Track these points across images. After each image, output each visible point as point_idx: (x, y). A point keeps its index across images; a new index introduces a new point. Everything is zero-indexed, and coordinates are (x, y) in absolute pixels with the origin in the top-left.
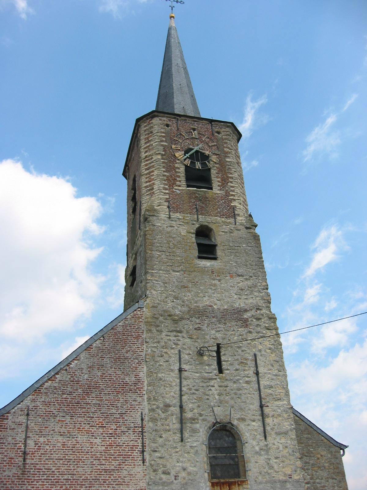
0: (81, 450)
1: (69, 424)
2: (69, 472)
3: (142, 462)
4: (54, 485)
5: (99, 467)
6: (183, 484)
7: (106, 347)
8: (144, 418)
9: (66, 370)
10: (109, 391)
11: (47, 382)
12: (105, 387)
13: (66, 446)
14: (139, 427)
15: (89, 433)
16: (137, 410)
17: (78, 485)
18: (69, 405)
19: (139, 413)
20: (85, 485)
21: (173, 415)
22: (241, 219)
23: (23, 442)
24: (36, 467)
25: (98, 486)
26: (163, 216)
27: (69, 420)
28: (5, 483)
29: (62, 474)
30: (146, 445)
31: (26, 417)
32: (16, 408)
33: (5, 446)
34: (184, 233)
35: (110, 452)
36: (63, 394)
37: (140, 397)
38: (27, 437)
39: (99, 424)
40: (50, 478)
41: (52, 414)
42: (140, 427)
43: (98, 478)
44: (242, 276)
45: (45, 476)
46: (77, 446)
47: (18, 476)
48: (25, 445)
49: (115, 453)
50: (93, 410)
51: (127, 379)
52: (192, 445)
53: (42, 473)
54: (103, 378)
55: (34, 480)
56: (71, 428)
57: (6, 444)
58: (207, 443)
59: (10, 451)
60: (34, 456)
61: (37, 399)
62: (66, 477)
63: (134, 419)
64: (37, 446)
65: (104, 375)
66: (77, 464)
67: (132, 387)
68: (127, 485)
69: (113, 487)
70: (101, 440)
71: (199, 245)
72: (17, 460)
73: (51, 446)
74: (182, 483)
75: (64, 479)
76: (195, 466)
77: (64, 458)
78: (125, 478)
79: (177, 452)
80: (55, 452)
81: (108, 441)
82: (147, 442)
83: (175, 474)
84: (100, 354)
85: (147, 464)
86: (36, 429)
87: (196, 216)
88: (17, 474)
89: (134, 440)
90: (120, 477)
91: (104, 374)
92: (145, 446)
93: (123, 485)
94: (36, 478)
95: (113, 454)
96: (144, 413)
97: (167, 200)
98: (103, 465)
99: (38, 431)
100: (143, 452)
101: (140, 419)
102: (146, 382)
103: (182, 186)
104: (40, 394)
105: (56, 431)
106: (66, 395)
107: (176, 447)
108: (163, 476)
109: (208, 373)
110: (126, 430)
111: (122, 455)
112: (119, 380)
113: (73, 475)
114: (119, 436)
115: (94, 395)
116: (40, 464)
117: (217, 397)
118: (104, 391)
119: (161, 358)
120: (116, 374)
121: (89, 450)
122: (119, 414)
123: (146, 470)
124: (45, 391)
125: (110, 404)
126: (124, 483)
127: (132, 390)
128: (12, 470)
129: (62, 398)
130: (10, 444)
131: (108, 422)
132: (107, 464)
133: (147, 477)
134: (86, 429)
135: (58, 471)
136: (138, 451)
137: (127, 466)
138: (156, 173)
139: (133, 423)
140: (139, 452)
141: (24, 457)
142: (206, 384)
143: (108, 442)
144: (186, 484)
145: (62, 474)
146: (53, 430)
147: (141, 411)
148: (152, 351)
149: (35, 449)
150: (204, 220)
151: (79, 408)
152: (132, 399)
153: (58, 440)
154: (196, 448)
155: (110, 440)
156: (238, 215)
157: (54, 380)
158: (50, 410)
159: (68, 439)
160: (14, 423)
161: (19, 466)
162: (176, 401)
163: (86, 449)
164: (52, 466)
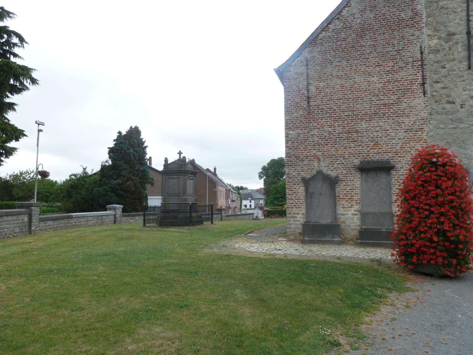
0: (359, 89)
1: (345, 68)
2: (349, 109)
3: (422, 94)
4: (336, 121)
5: (378, 102)
8: (423, 51)
9: (338, 18)
10: (384, 31)
11: (320, 33)
12: (379, 27)
13: (344, 87)
14: (418, 61)
15: (366, 73)
16: (416, 44)
17: (358, 119)
18: (344, 51)
19: (418, 47)
20: (365, 119)
21: (457, 43)
23: (306, 89)
24: (319, 107)
25: (378, 119)
28: (294, 122)
29: (343, 112)
30: (427, 77)
31: (305, 67)
32: (296, 61)
33: (291, 93)
35: (388, 87)
36: (337, 41)
37: (418, 30)
38: (308, 84)
39: (375, 64)
40: (333, 115)
41: (329, 61)
42: (420, 61)
43: (377, 112)
45: (328, 114)
46: (355, 86)
47: (305, 117)
48: (308, 90)
49: (393, 88)
50: (368, 52)
51: (403, 15)
53: (324, 112)
54: (376, 19)
55: (319, 118)
56: (347, 71)
57: (292, 92)
59: (296, 97)
60: (317, 99)
61: (314, 50)
62: (347, 114)
63: (413, 54)
64: (318, 90)
65: (377, 16)
66: (356, 102)
67: (408, 22)
68: (407, 116)
69: (393, 119)
70: (378, 78)
72: (302, 104)
73: (331, 89)
75: (345, 116)
77: (343, 98)
78: (405, 110)
79: (464, 81)
80: (334, 93)
81: (386, 78)
82: (428, 74)
83: (461, 103)
85: (429, 95)
86: (316, 76)
88: (304, 115)
89: (413, 74)
90: (400, 109)
91: (378, 15)
92: (426, 79)
93: (403, 116)
94: (320, 117)
96: (423, 47)
98: (382, 100)
99: (318, 77)
100: (423, 84)
101: (419, 52)
102: (425, 14)
104: (316, 46)
105: (334, 74)
106: (340, 42)
107: (462, 76)
108: (448, 106)
110: (404, 65)
111: (401, 89)
112: (393, 17)
113: (353, 111)
114: (397, 72)
115: (368, 37)
116: (322, 105)
118: (378, 32)
120: (390, 13)
121: (366, 88)
122: (395, 51)
123: (427, 101)
124: (321, 41)
125: (385, 43)
126: (404, 115)
127: (409, 25)
128: (299, 112)
129: (337, 45)
130: (295, 91)
131: (385, 60)
132: (385, 99)
133: (429, 108)
134: (362, 70)
135: (339, 109)
136: (418, 84)
137: (407, 99)
140: (419, 85)
141: (308, 100)
143: (385, 79)
145: (343, 112)
146: (331, 75)
147: (420, 44)
149: (316, 93)
151: (354, 51)
152: (409, 35)
153: (336, 83)
155: (388, 77)
157: (327, 31)
158: (326, 58)
159: (346, 81)
160: (296, 74)
161: (304, 109)
164: (333, 105)
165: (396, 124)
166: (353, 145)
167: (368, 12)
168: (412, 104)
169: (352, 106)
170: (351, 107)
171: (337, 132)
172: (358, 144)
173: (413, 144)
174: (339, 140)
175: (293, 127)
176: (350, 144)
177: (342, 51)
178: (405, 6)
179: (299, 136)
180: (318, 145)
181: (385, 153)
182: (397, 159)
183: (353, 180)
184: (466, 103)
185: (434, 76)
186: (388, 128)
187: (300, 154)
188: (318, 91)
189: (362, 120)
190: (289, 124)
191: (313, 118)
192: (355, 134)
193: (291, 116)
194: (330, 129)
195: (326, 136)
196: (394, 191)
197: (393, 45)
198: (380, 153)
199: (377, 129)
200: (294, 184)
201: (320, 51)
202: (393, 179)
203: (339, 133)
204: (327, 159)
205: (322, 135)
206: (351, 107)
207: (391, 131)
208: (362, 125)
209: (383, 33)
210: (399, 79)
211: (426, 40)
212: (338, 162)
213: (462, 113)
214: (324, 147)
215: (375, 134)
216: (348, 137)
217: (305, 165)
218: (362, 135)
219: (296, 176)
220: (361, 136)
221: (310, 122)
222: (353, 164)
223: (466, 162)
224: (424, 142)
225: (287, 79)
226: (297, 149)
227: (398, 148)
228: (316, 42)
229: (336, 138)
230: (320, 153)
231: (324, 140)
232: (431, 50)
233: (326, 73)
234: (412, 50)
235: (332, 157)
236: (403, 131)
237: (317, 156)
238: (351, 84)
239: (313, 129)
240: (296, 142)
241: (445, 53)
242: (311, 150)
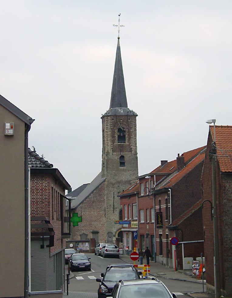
22: (133, 152)
26: (111, 154)
34: (116, 158)
38: (81, 213)
44: (131, 170)
71: (120, 162)
87: (120, 153)
97: (112, 149)
100: (105, 215)
103: (116, 143)
138: (109, 139)
150: (122, 154)
156: (132, 151)
162: (113, 204)
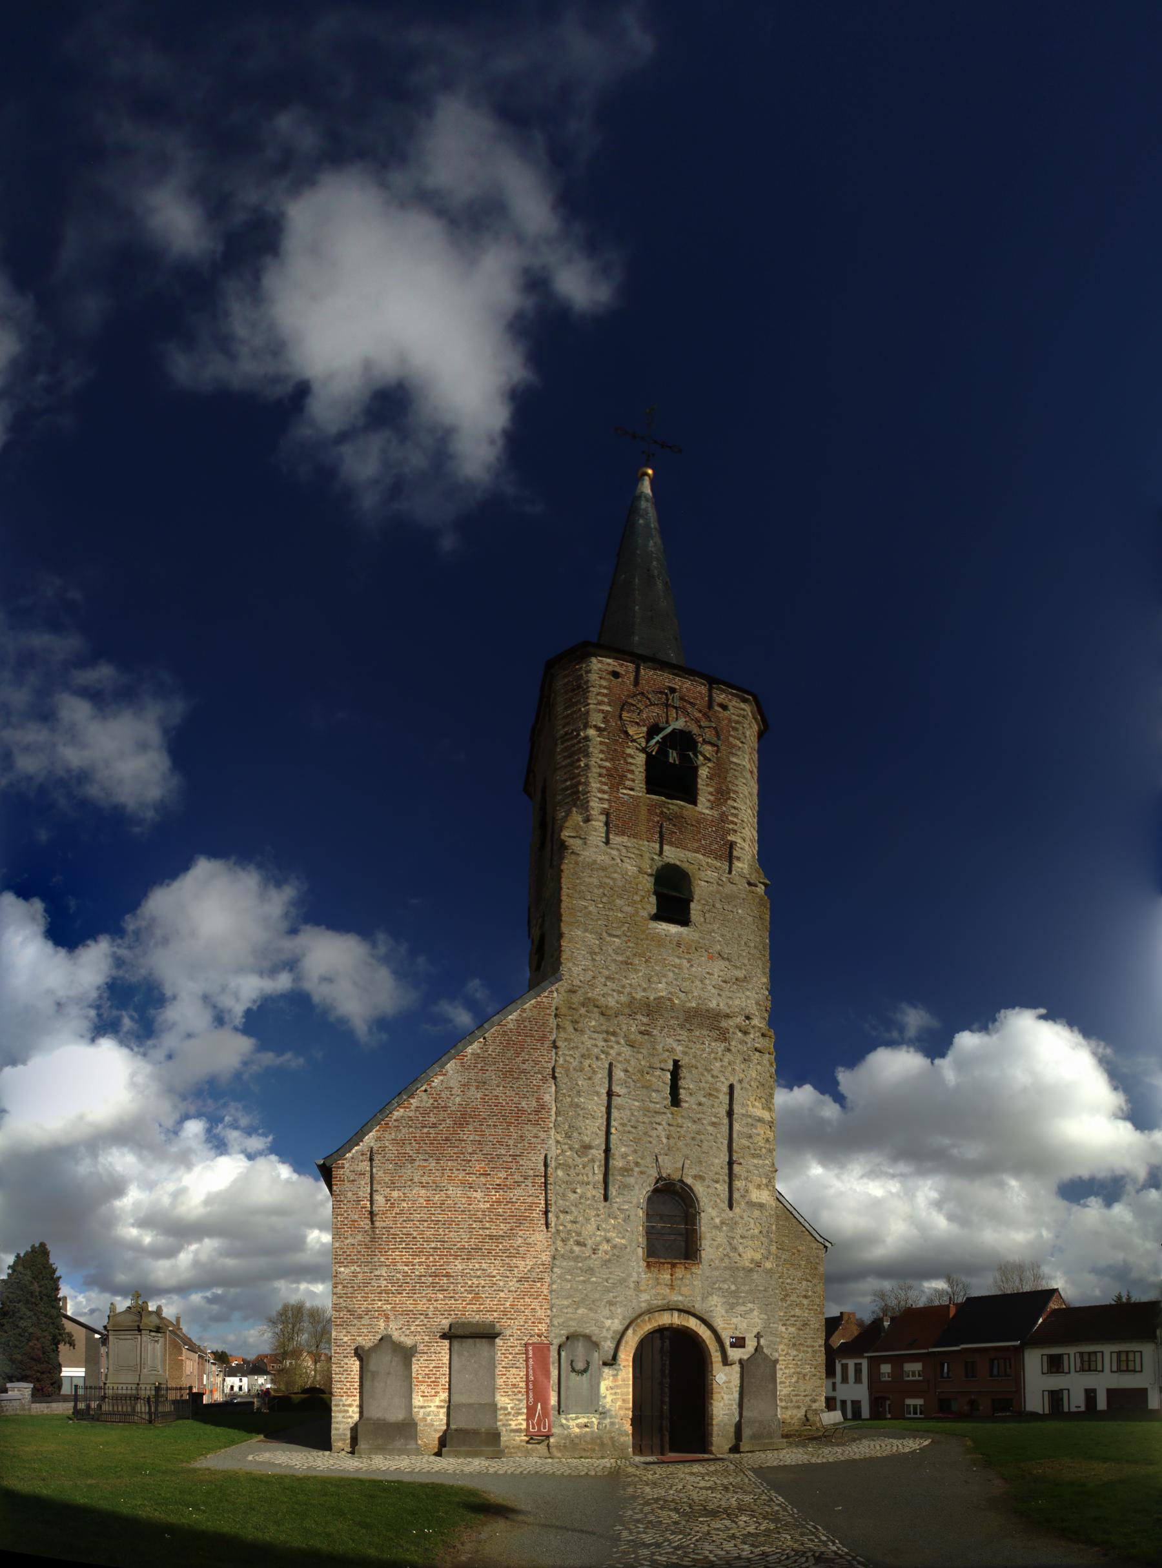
4: (417, 1255)
5: (481, 1232)
6: (606, 1261)
7: (489, 1054)
9: (426, 1091)
12: (489, 1115)
16: (539, 1150)
17: (450, 1255)
18: (433, 1144)
19: (542, 1157)
20: (461, 1256)
27: (434, 1165)
28: (348, 1253)
30: (552, 1202)
32: (354, 1151)
33: (344, 1204)
36: (423, 1127)
37: (544, 1131)
39: (479, 1171)
40: (411, 1246)
47: (365, 1245)
48: (372, 1201)
51: (523, 1104)
52: (622, 1207)
53: (398, 1240)
55: (389, 1249)
56: (437, 1177)
58: (645, 1206)
60: (386, 1217)
61: (384, 1137)
62: (433, 1245)
65: (487, 1098)
67: (531, 1116)
68: (522, 1257)
69: (502, 1260)
70: (483, 1193)
72: (362, 1223)
74: (604, 1259)
75: (430, 1248)
76: (623, 1238)
78: (520, 1249)
79: (598, 1215)
84: (479, 1065)
86: (387, 1179)
92: (551, 1204)
93: (516, 1257)
95: (501, 1214)
98: (487, 1229)
100: (546, 1213)
101: (542, 1164)
102: (554, 1109)
105: (416, 1180)
108: (576, 1249)
109: (654, 1102)
110: (521, 1179)
113: (444, 1242)
114: (511, 1189)
117: (665, 1141)
119: (579, 1073)
120: (506, 1096)
122: (510, 1155)
124: (396, 1124)
137: (523, 1232)
139: (532, 1169)
142: (650, 1119)
143: (494, 1197)
144: (609, 1260)
145: (427, 1241)
146: (411, 1180)
147: (546, 1152)
148: (565, 1061)
151: (448, 1147)
154: (627, 1213)
157: (408, 1108)
159: (434, 1192)
161: (366, 1232)
162: (600, 1141)
163: (462, 1206)
165: (505, 1268)
166: (441, 1296)
167: (473, 1089)
168: (530, 1240)
169: (443, 1233)
170: (440, 1235)
171: (417, 1273)
172: (449, 1295)
173: (529, 1300)
174: (420, 1286)
175: (345, 1261)
176: (436, 1294)
177: (430, 1144)
178: (527, 1091)
179: (355, 1276)
180: (385, 1293)
181: (488, 1311)
182: (506, 1322)
183: (440, 1353)
184: (601, 1247)
185: (561, 1202)
186: (494, 1273)
187: (357, 1306)
188: (389, 1205)
189: (456, 1257)
190: (340, 1255)
191: (379, 1248)
192: (445, 1278)
193: (342, 1242)
194: (406, 1268)
195: (399, 1279)
196: (501, 1371)
197: (507, 1146)
198: (482, 1311)
199: (479, 1273)
200: (344, 1357)
201: (395, 1140)
202: (499, 1352)
203: (421, 1276)
204: (400, 1316)
205: (393, 1276)
206: (440, 1235)
207: (498, 1278)
208: (456, 1266)
209: (494, 1125)
210: (514, 1200)
211: (554, 1148)
212: (417, 1323)
213: (594, 1262)
214: (396, 1297)
215: (474, 1280)
216: (433, 1283)
217: (363, 1325)
218: (454, 1281)
219: (349, 1344)
220: (453, 1283)
221: (375, 1255)
222: (440, 1327)
223: (596, 1332)
224: (543, 1299)
225: (338, 1181)
226: (352, 1297)
227: (508, 1304)
228: (388, 1124)
229: (416, 1283)
230: (389, 1307)
231: (396, 1285)
232: (560, 1164)
233: (402, 1176)
234: (533, 1159)
235: (409, 1314)
236: (515, 1279)
237: (383, 1311)
238: (441, 1199)
239: (379, 1266)
240: (349, 1285)
241: (577, 1171)
242: (374, 1300)
